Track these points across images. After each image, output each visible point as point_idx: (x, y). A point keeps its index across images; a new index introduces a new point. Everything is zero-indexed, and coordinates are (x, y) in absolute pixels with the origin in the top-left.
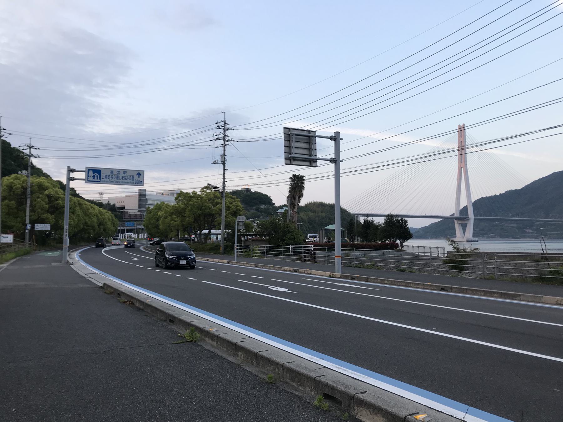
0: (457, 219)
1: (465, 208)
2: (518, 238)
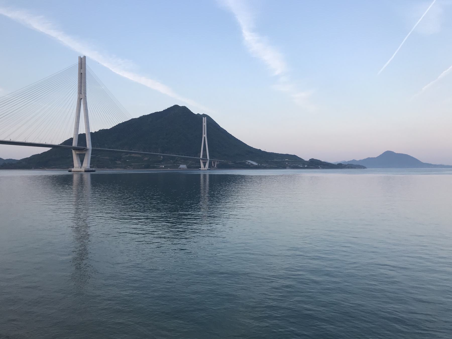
0: (75, 149)
2: (111, 168)
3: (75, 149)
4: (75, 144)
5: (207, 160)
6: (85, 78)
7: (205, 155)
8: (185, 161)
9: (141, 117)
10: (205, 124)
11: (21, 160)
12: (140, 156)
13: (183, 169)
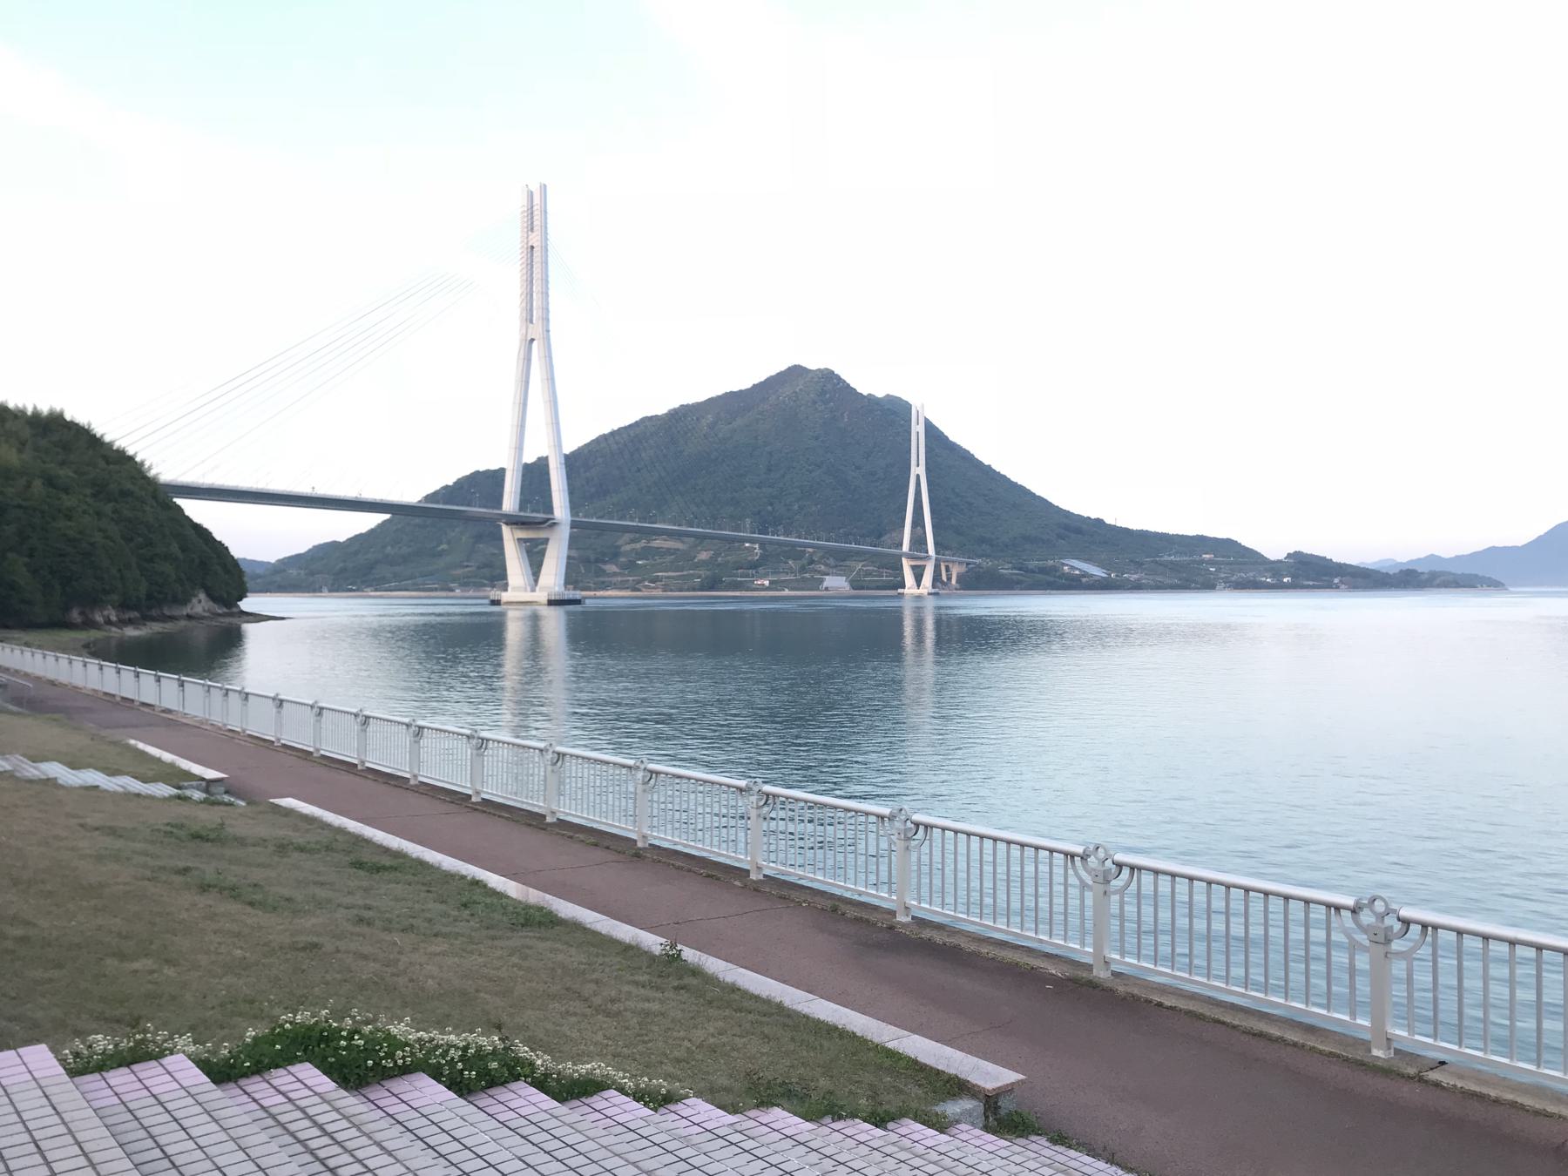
3: (515, 522)
4: (510, 503)
5: (928, 558)
6: (545, 263)
7: (919, 542)
8: (839, 561)
11: (281, 562)
12: (679, 545)
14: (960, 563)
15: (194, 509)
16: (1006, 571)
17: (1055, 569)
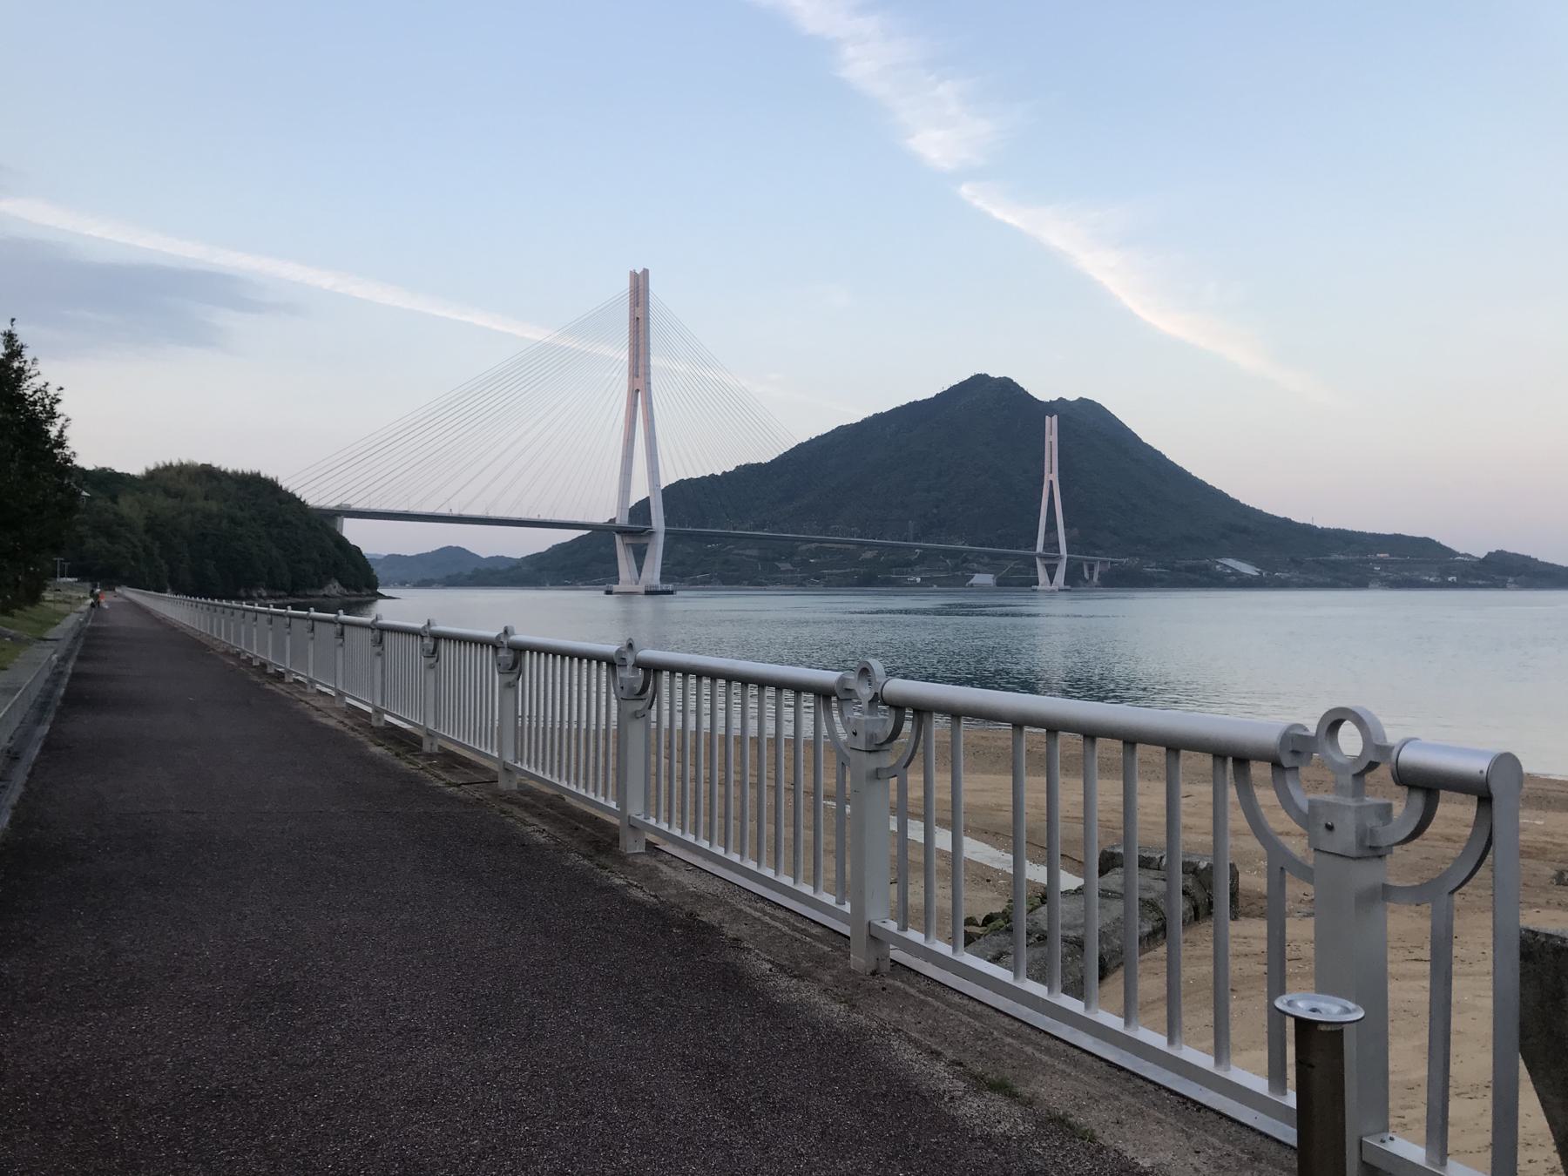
0: (623, 531)
1: (644, 505)
5: (1060, 558)
9: (865, 421)
10: (1052, 438)
13: (983, 589)
14: (1103, 562)
15: (353, 531)
16: (1150, 569)
17: (1207, 568)
